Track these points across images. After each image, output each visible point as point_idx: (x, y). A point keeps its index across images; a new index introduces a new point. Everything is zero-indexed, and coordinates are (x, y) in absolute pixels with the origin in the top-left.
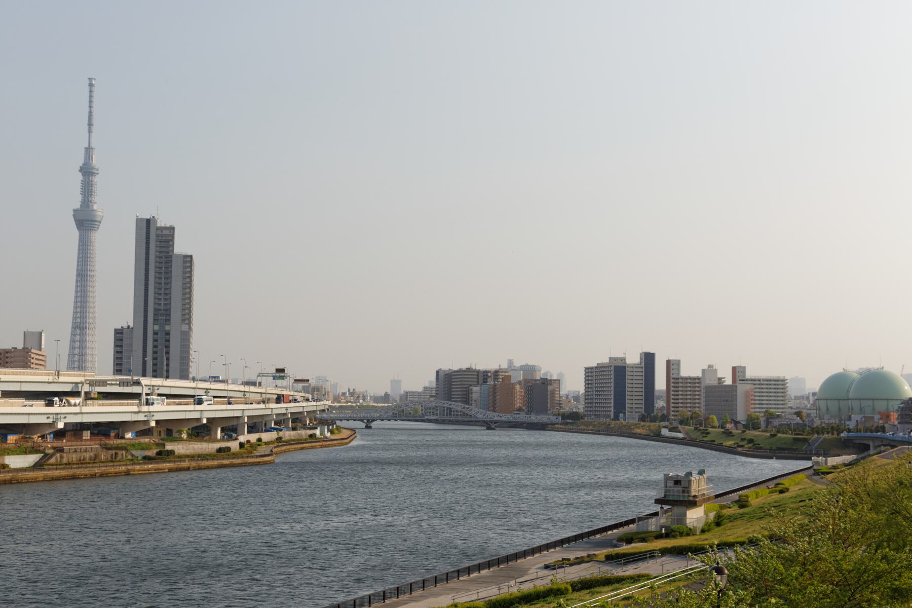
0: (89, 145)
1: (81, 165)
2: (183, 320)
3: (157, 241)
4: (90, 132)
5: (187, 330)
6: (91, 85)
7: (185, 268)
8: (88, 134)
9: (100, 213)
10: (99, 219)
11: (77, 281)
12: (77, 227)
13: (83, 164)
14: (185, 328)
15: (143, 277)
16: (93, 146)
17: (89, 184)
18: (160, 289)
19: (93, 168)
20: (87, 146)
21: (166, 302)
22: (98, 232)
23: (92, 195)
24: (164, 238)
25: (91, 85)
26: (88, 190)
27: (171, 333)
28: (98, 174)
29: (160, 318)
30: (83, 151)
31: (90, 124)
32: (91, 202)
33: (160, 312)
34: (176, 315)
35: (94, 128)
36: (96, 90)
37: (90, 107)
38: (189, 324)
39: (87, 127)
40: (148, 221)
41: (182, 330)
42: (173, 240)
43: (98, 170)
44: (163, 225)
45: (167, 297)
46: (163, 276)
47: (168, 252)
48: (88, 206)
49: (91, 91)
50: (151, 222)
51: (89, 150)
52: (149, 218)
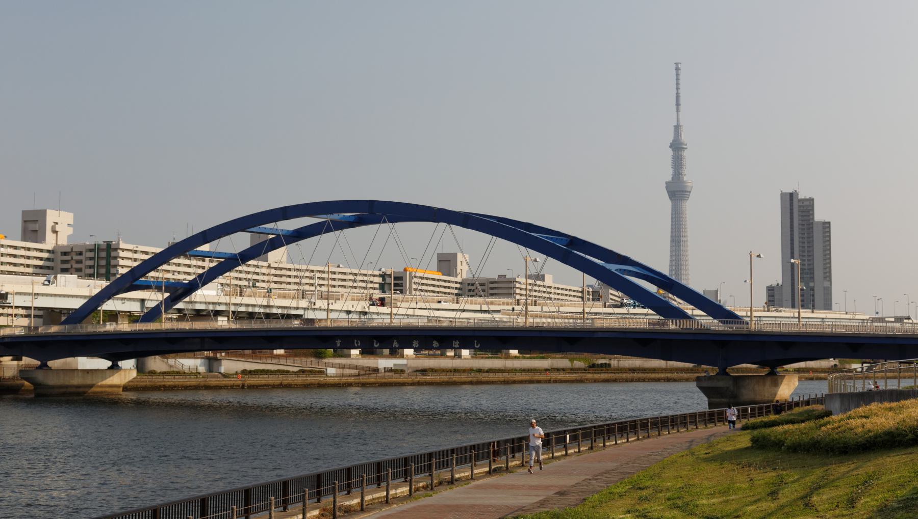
0: (678, 123)
1: (671, 142)
2: (825, 278)
3: (799, 212)
4: (678, 111)
5: (829, 286)
6: (677, 69)
7: (824, 233)
8: (676, 113)
9: (689, 184)
10: (689, 190)
11: (671, 247)
12: (670, 198)
13: (673, 141)
14: (826, 284)
15: (789, 242)
16: (681, 123)
17: (678, 158)
18: (804, 251)
19: (682, 144)
20: (676, 124)
21: (809, 263)
22: (688, 201)
23: (682, 168)
24: (805, 208)
25: (677, 69)
26: (679, 164)
27: (815, 289)
28: (686, 149)
29: (805, 276)
30: (672, 129)
31: (678, 105)
32: (681, 174)
33: (805, 271)
34: (818, 273)
35: (682, 108)
36: (682, 73)
37: (678, 89)
38: (830, 281)
39: (675, 107)
40: (791, 195)
41: (825, 286)
42: (813, 210)
43: (686, 145)
44: (803, 198)
45: (810, 258)
46: (806, 240)
47: (809, 220)
48: (679, 178)
49: (677, 75)
50: (794, 196)
51: (677, 128)
52: (791, 192)
